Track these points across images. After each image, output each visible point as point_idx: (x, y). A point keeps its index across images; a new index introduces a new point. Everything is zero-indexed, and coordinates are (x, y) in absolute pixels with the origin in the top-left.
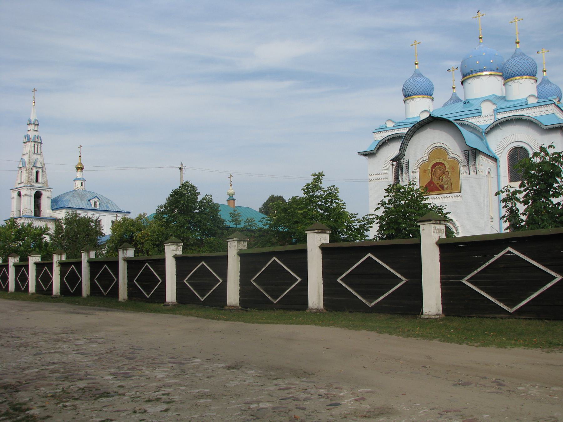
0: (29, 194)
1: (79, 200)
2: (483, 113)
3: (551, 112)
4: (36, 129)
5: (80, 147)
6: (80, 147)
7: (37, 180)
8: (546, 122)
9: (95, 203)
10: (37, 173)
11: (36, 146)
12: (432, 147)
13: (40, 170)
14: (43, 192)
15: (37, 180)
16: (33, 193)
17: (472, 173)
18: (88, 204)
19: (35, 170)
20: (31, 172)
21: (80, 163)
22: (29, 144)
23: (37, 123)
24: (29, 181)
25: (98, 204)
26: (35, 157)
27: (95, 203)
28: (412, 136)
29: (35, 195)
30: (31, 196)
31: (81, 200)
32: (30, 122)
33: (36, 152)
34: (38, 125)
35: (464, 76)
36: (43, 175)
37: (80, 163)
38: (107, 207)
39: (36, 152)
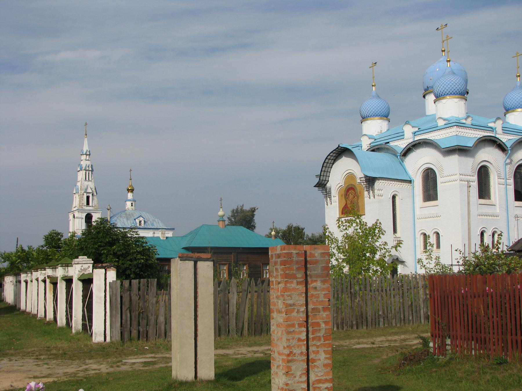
0: (80, 216)
1: (125, 220)
2: (406, 137)
3: (454, 134)
4: (87, 159)
5: (131, 171)
6: (131, 171)
7: (88, 203)
8: (444, 145)
9: (140, 222)
10: (88, 198)
11: (87, 174)
12: (345, 174)
13: (91, 195)
14: (93, 214)
15: (88, 203)
16: (84, 215)
17: (372, 197)
18: (133, 223)
19: (85, 196)
20: (83, 197)
21: (131, 186)
22: (81, 172)
23: (88, 153)
24: (81, 205)
25: (143, 222)
26: (86, 183)
27: (140, 222)
28: (333, 164)
29: (86, 216)
30: (82, 218)
31: (127, 219)
32: (83, 152)
33: (87, 179)
34: (89, 155)
35: (426, 90)
36: (93, 199)
37: (131, 186)
38: (152, 224)
39: (87, 179)
